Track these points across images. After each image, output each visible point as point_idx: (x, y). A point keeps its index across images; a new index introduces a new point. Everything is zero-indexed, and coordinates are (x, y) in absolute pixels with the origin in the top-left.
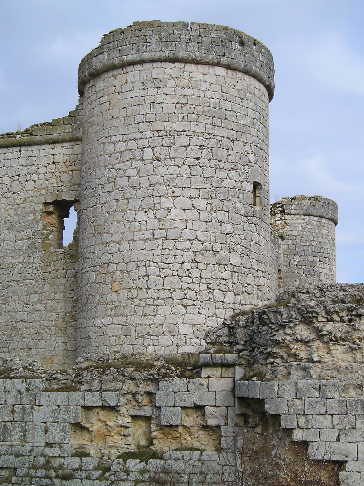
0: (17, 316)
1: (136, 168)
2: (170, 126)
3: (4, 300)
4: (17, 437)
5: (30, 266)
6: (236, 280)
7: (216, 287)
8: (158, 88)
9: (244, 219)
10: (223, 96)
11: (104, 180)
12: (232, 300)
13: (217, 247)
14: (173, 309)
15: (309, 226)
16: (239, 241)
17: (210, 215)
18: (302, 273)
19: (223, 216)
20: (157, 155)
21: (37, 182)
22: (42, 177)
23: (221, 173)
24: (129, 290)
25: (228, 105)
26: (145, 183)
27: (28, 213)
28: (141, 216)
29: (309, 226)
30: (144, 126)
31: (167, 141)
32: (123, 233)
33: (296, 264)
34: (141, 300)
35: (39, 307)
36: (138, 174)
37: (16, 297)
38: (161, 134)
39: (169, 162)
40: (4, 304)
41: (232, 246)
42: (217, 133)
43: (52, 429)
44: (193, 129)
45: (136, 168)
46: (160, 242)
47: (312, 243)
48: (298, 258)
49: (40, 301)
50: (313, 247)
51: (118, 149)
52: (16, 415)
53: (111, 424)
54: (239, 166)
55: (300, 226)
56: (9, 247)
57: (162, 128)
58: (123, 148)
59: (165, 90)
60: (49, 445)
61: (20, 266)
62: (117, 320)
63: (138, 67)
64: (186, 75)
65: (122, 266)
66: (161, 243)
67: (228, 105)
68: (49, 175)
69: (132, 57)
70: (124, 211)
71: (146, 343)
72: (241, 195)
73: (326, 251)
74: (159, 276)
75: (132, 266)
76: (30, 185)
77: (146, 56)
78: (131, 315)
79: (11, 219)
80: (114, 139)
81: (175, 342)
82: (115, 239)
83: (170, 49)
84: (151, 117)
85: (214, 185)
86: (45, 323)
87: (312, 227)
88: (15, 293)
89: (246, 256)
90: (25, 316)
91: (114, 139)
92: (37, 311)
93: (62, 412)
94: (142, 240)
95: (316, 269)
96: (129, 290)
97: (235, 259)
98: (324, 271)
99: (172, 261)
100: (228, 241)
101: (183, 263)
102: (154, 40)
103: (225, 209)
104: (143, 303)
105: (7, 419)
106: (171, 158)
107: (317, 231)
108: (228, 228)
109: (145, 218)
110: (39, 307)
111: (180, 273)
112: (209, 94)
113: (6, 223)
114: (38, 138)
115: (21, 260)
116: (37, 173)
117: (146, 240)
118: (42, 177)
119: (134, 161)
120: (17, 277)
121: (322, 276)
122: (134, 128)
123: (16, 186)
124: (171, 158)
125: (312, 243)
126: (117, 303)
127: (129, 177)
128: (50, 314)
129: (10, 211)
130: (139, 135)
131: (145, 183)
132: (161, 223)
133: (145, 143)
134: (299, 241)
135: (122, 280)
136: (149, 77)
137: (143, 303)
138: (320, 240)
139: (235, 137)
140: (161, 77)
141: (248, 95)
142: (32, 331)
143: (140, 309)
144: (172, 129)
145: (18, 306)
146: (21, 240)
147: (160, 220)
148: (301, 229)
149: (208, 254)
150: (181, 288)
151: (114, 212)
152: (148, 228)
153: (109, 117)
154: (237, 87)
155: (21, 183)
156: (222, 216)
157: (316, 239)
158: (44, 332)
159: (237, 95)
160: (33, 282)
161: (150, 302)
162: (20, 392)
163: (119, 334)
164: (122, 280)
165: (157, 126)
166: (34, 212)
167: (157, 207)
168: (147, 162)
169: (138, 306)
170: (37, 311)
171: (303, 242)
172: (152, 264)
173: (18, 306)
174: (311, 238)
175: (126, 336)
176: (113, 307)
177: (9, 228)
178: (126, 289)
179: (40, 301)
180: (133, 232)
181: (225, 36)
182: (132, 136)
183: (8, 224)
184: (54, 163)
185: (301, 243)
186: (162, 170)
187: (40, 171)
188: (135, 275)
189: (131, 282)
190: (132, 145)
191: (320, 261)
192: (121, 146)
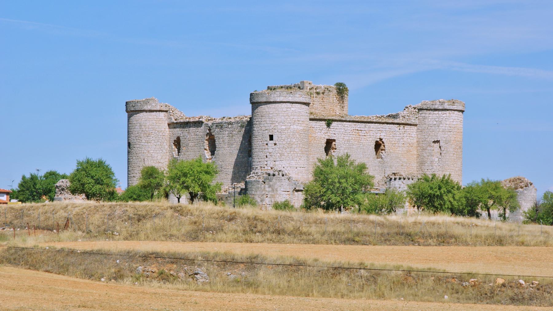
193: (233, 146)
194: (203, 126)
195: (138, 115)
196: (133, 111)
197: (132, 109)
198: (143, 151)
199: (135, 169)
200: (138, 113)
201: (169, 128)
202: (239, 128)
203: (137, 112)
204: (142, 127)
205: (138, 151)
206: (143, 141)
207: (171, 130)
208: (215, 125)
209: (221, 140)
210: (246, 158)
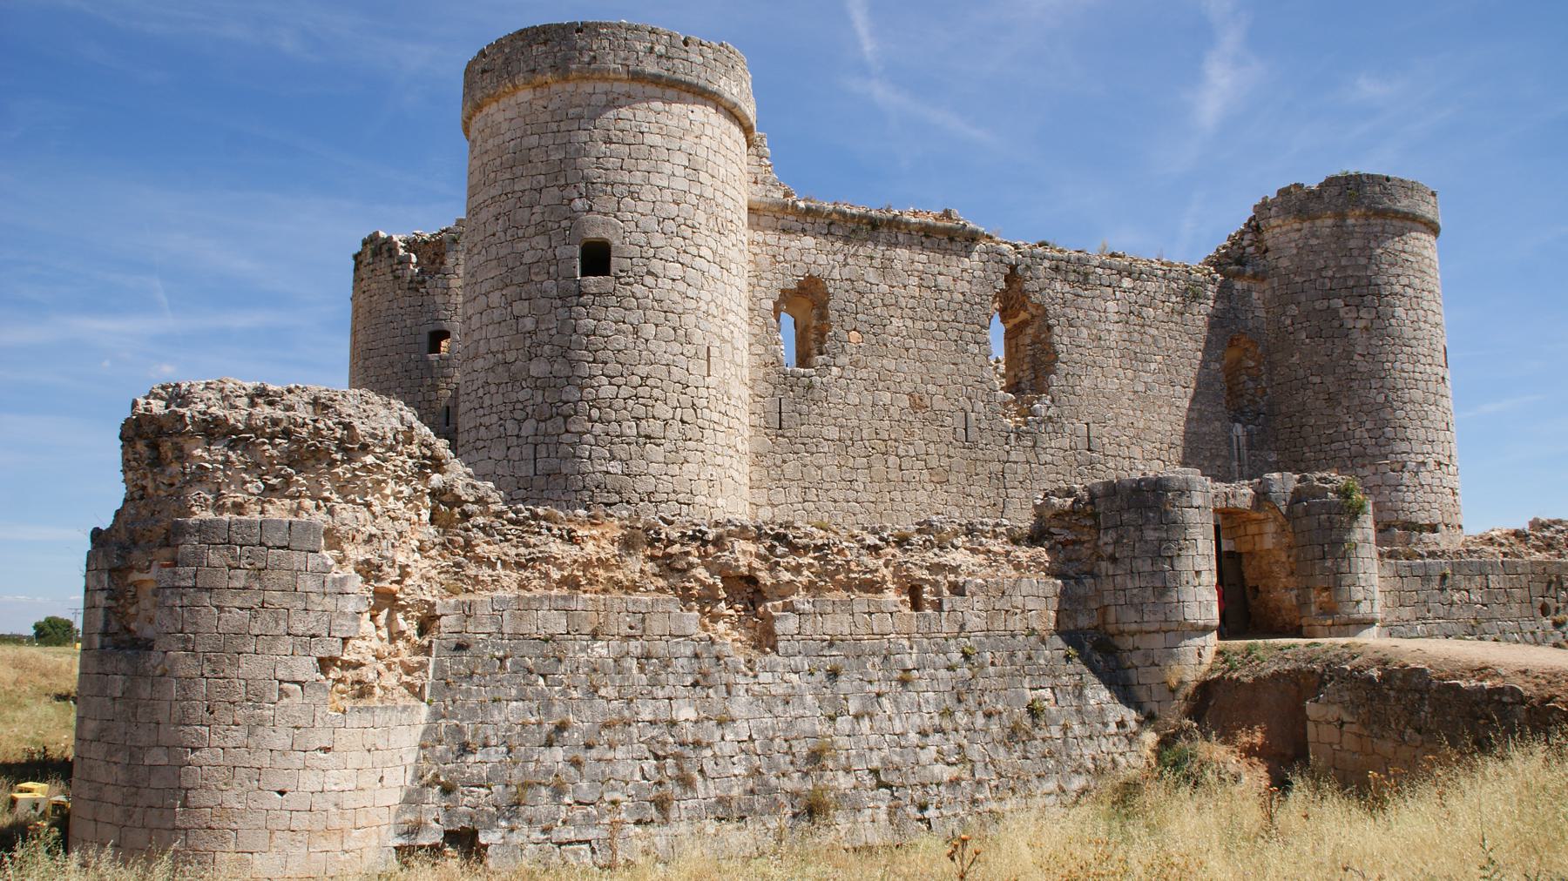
6: (540, 399)
7: (508, 414)
9: (559, 302)
10: (525, 131)
12: (532, 432)
13: (510, 357)
15: (1314, 242)
16: (546, 339)
17: (504, 312)
18: (1304, 337)
19: (520, 307)
23: (520, 245)
25: (534, 140)
29: (1314, 242)
33: (1288, 322)
41: (533, 350)
42: (516, 188)
44: (493, 192)
47: (1324, 274)
48: (1293, 310)
50: (1327, 280)
54: (550, 224)
55: (1293, 245)
67: (534, 140)
72: (552, 269)
73: (1364, 282)
85: (510, 266)
87: (1320, 241)
89: (560, 360)
95: (1336, 323)
97: (538, 368)
98: (1361, 324)
100: (528, 343)
103: (523, 296)
107: (1333, 246)
108: (529, 323)
112: (508, 136)
121: (1355, 334)
125: (1324, 274)
134: (1292, 276)
138: (1344, 262)
139: (543, 182)
141: (571, 111)
148: (1295, 251)
149: (500, 369)
154: (550, 108)
156: (520, 308)
157: (1332, 263)
159: (549, 119)
171: (1301, 274)
174: (1320, 263)
181: (521, 43)
185: (1297, 279)
191: (1346, 305)
193: (1153, 366)
194: (975, 256)
195: (677, 108)
196: (656, 80)
197: (651, 67)
198: (704, 307)
199: (656, 393)
200: (680, 100)
201: (751, 226)
202: (1173, 299)
203: (670, 93)
204: (703, 177)
205: (677, 297)
206: (705, 251)
207: (759, 236)
208: (1047, 263)
209: (1085, 332)
210: (1218, 424)
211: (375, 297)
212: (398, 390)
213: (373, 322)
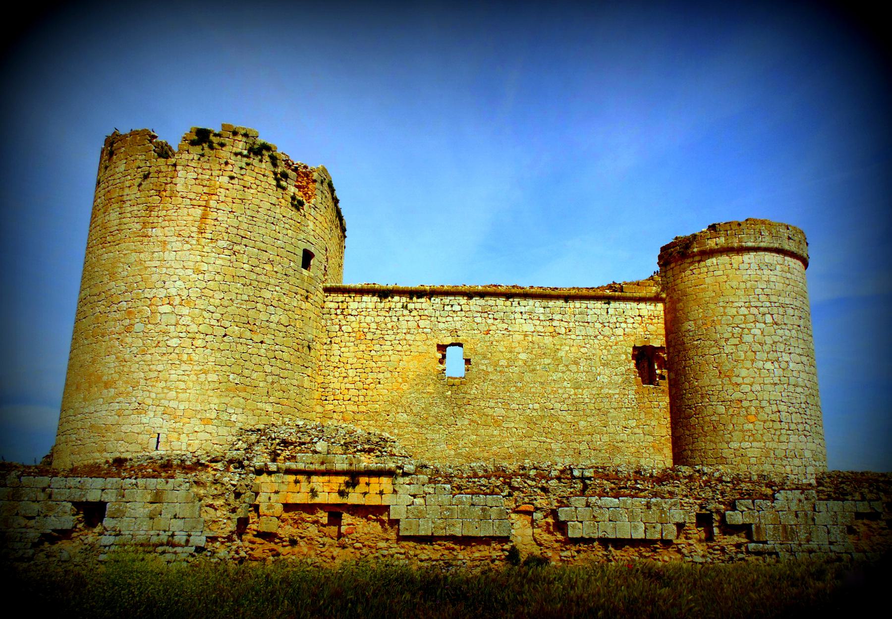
0: (618, 438)
1: (760, 329)
2: (782, 300)
3: (604, 424)
4: (803, 537)
5: (626, 396)
8: (771, 270)
11: (726, 335)
14: (800, 438)
20: (776, 320)
21: (626, 329)
22: (630, 326)
24: (765, 422)
26: (769, 340)
27: (620, 354)
28: (768, 365)
30: (762, 298)
31: (781, 310)
32: (754, 378)
34: (776, 430)
35: (637, 430)
36: (762, 333)
37: (615, 422)
38: (777, 305)
39: (784, 327)
40: (605, 427)
43: (832, 530)
45: (760, 329)
46: (786, 386)
49: (638, 426)
51: (741, 313)
52: (800, 520)
53: (875, 526)
56: (606, 381)
57: (777, 301)
58: (746, 312)
59: (775, 272)
60: (831, 543)
61: (617, 396)
62: (755, 444)
63: (752, 254)
64: (786, 262)
65: (755, 403)
66: (786, 387)
68: (636, 325)
69: (750, 244)
70: (753, 361)
71: (784, 464)
74: (788, 412)
75: (764, 404)
76: (619, 332)
77: (762, 245)
78: (769, 442)
79: (605, 358)
80: (736, 304)
81: (804, 463)
82: (746, 381)
83: (779, 242)
84: (767, 291)
86: (644, 444)
88: (614, 418)
90: (625, 438)
91: (736, 304)
92: (635, 434)
93: (839, 517)
94: (772, 384)
96: (765, 422)
99: (794, 401)
101: (801, 403)
102: (767, 234)
104: (778, 433)
105: (792, 523)
106: (785, 324)
109: (773, 368)
110: (637, 430)
111: (801, 410)
113: (601, 361)
114: (628, 295)
115: (617, 391)
116: (625, 322)
117: (776, 384)
118: (630, 326)
119: (757, 324)
120: (615, 405)
122: (754, 298)
123: (607, 331)
124: (785, 324)
126: (754, 432)
127: (755, 335)
128: (647, 437)
129: (604, 351)
130: (759, 304)
131: (769, 340)
132: (785, 372)
133: (766, 310)
135: (757, 413)
136: (763, 261)
137: (778, 433)
140: (771, 261)
142: (633, 450)
143: (776, 437)
144: (783, 302)
145: (618, 429)
146: (616, 375)
147: (784, 369)
150: (802, 423)
151: (743, 360)
152: (776, 375)
153: (728, 287)
155: (612, 328)
158: (643, 451)
160: (630, 410)
161: (784, 432)
162: (800, 501)
163: (759, 456)
164: (757, 413)
165: (773, 299)
166: (626, 354)
167: (780, 359)
168: (769, 325)
169: (775, 434)
170: (635, 434)
172: (782, 403)
173: (618, 429)
175: (766, 457)
176: (750, 434)
177: (604, 365)
178: (762, 421)
179: (638, 426)
180: (763, 377)
182: (753, 304)
183: (603, 361)
184: (639, 316)
186: (780, 332)
187: (628, 321)
188: (768, 410)
189: (766, 415)
190: (754, 311)
192: (744, 311)
211: (252, 191)
212: (277, 288)
213: (249, 212)
